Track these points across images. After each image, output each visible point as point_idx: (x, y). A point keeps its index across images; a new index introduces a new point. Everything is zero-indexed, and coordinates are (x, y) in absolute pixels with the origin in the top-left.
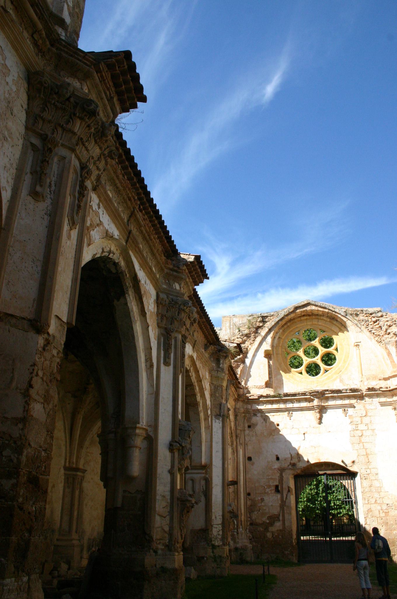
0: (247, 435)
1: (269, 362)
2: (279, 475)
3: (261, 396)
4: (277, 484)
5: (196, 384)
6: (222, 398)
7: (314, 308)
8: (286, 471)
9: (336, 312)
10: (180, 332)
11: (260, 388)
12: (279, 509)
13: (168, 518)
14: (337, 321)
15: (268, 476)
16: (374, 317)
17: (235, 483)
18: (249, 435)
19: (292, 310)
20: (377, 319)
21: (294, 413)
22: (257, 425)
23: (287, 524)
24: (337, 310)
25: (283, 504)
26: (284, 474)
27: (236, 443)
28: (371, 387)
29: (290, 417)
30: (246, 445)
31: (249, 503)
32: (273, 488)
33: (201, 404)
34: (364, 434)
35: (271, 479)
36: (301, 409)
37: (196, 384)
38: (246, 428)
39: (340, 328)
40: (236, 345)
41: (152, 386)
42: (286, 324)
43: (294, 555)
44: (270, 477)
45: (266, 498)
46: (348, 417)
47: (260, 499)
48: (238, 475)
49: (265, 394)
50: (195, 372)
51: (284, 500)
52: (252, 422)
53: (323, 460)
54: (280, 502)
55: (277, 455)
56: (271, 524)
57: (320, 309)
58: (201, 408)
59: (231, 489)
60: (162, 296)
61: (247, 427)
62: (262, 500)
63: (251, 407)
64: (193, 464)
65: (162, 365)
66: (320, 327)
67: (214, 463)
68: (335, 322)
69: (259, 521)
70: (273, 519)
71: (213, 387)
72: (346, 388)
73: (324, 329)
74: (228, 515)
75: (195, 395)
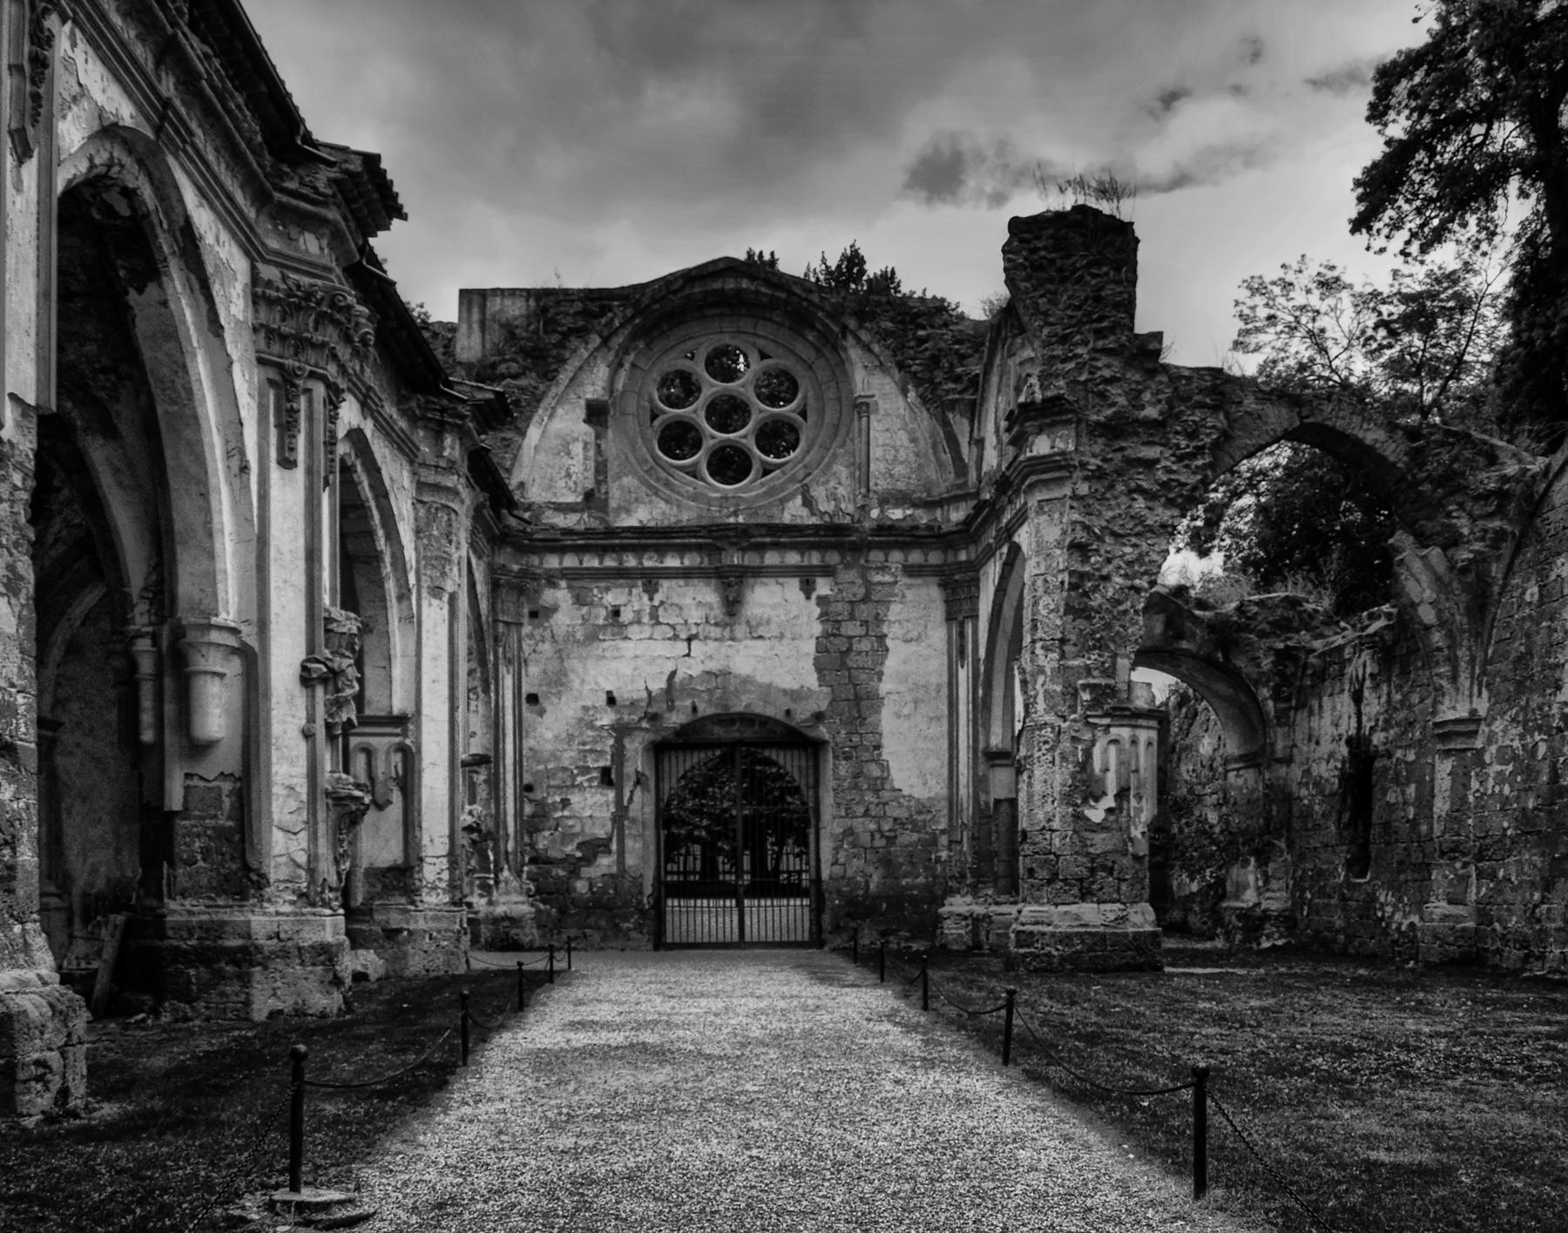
5: (372, 504)
6: (450, 542)
9: (811, 302)
10: (323, 378)
12: (609, 824)
18: (531, 636)
21: (665, 584)
27: (496, 657)
33: (387, 559)
37: (372, 504)
39: (818, 350)
40: (490, 396)
47: (558, 799)
53: (739, 706)
55: (609, 693)
58: (387, 568)
60: (269, 272)
64: (368, 712)
65: (273, 465)
67: (425, 710)
71: (422, 512)
74: (463, 840)
75: (370, 534)
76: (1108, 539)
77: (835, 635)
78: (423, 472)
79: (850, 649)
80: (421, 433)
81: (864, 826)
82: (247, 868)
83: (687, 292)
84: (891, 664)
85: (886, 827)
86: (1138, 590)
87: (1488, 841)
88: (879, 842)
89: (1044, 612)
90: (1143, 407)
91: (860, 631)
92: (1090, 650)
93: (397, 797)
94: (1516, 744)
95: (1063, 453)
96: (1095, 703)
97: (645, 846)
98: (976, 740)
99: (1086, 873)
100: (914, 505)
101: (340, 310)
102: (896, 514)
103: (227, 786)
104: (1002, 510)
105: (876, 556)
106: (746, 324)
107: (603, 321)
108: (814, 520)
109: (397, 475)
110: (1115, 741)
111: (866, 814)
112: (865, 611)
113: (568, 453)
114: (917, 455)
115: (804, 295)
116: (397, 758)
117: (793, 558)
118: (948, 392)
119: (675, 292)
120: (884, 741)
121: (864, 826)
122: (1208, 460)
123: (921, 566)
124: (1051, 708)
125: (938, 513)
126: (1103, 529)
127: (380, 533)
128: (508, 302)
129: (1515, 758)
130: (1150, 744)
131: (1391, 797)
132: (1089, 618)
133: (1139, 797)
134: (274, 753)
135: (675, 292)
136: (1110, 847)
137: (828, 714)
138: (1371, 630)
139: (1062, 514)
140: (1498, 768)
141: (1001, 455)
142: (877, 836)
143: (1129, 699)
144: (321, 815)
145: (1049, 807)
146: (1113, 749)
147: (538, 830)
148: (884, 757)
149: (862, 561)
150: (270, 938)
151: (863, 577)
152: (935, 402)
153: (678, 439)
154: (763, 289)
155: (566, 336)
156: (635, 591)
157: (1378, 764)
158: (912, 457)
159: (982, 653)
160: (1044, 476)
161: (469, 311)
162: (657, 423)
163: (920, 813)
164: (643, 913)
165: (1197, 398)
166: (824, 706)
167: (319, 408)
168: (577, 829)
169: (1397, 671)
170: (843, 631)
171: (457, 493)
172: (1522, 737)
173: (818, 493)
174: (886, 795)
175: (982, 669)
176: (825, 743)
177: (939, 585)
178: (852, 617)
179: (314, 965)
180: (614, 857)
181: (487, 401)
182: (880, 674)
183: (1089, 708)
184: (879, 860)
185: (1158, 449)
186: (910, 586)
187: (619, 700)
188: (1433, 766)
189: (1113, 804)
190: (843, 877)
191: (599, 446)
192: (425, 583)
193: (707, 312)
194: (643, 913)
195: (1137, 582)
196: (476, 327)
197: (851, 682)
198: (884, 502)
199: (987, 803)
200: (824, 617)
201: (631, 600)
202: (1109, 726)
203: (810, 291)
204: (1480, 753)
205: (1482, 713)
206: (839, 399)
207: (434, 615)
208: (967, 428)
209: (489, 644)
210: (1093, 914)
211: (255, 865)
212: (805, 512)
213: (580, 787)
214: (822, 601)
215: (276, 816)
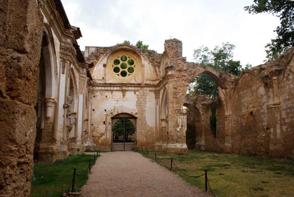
1: (105, 69)
2: (105, 117)
3: (100, 84)
4: (104, 121)
5: (73, 79)
7: (127, 47)
8: (109, 116)
10: (69, 60)
11: (100, 80)
12: (105, 130)
13: (62, 133)
14: (136, 54)
17: (87, 120)
19: (117, 47)
21: (114, 92)
22: (97, 96)
23: (108, 137)
24: (137, 50)
26: (107, 117)
28: (146, 83)
29: (112, 93)
31: (92, 128)
32: (103, 122)
33: (75, 88)
34: (142, 103)
36: (117, 90)
37: (73, 79)
38: (93, 97)
40: (91, 63)
41: (57, 82)
45: (99, 126)
46: (136, 95)
48: (88, 117)
49: (102, 83)
50: (73, 75)
53: (124, 112)
54: (105, 128)
56: (101, 137)
57: (129, 48)
59: (86, 122)
60: (63, 44)
65: (61, 74)
66: (129, 56)
67: (79, 112)
68: (136, 55)
69: (96, 135)
70: (102, 134)
72: (137, 83)
73: (130, 56)
74: (84, 133)
76: (179, 87)
78: (80, 74)
80: (80, 68)
81: (143, 131)
82: (53, 138)
83: (118, 48)
84: (147, 105)
85: (146, 131)
86: (183, 95)
87: (233, 134)
88: (145, 134)
89: (170, 98)
90: (184, 68)
91: (142, 100)
92: (177, 104)
93: (74, 126)
94: (236, 119)
95: (173, 74)
96: (178, 112)
97: (110, 134)
98: (159, 117)
99: (177, 139)
100: (150, 81)
101: (72, 50)
103: (51, 125)
105: (145, 88)
106: (127, 53)
107: (106, 52)
109: (77, 74)
110: (181, 118)
111: (143, 129)
112: (143, 97)
113: (100, 71)
116: (74, 120)
117: (133, 88)
119: (117, 48)
120: (146, 118)
121: (143, 131)
122: (193, 76)
123: (151, 90)
124: (172, 113)
126: (179, 85)
127: (74, 84)
128: (93, 48)
129: (236, 121)
130: (186, 118)
131: (219, 127)
132: (177, 99)
133: (184, 127)
134: (59, 119)
135: (117, 48)
136: (180, 135)
138: (215, 101)
140: (234, 122)
141: (163, 74)
143: (183, 112)
144: (65, 130)
145: (171, 128)
146: (180, 119)
147: (93, 131)
148: (146, 120)
149: (143, 89)
150: (56, 150)
151: (143, 92)
152: (154, 66)
153: (116, 70)
155: (101, 54)
156: (109, 93)
158: (150, 74)
161: (87, 50)
162: (113, 67)
163: (151, 129)
164: (109, 145)
165: (191, 67)
166: (137, 112)
167: (68, 64)
168: (100, 131)
169: (219, 107)
170: (140, 100)
171: (85, 78)
172: (237, 118)
173: (137, 79)
174: (146, 126)
175: (160, 106)
176: (137, 118)
178: (141, 98)
179: (63, 154)
180: (105, 136)
181: (90, 64)
182: (145, 107)
183: (177, 113)
184: (145, 137)
186: (150, 93)
187: (106, 110)
188: (224, 122)
189: (181, 128)
190: (140, 139)
191: (105, 70)
192: (80, 92)
193: (121, 51)
194: (109, 145)
195: (183, 94)
196: (87, 52)
198: (146, 80)
200: (137, 98)
201: (108, 94)
202: (180, 116)
203: (136, 48)
204: (231, 120)
205: (231, 114)
207: (81, 97)
208: (158, 70)
209: (87, 101)
210: (179, 146)
211: (54, 138)
214: (137, 95)
215: (58, 130)
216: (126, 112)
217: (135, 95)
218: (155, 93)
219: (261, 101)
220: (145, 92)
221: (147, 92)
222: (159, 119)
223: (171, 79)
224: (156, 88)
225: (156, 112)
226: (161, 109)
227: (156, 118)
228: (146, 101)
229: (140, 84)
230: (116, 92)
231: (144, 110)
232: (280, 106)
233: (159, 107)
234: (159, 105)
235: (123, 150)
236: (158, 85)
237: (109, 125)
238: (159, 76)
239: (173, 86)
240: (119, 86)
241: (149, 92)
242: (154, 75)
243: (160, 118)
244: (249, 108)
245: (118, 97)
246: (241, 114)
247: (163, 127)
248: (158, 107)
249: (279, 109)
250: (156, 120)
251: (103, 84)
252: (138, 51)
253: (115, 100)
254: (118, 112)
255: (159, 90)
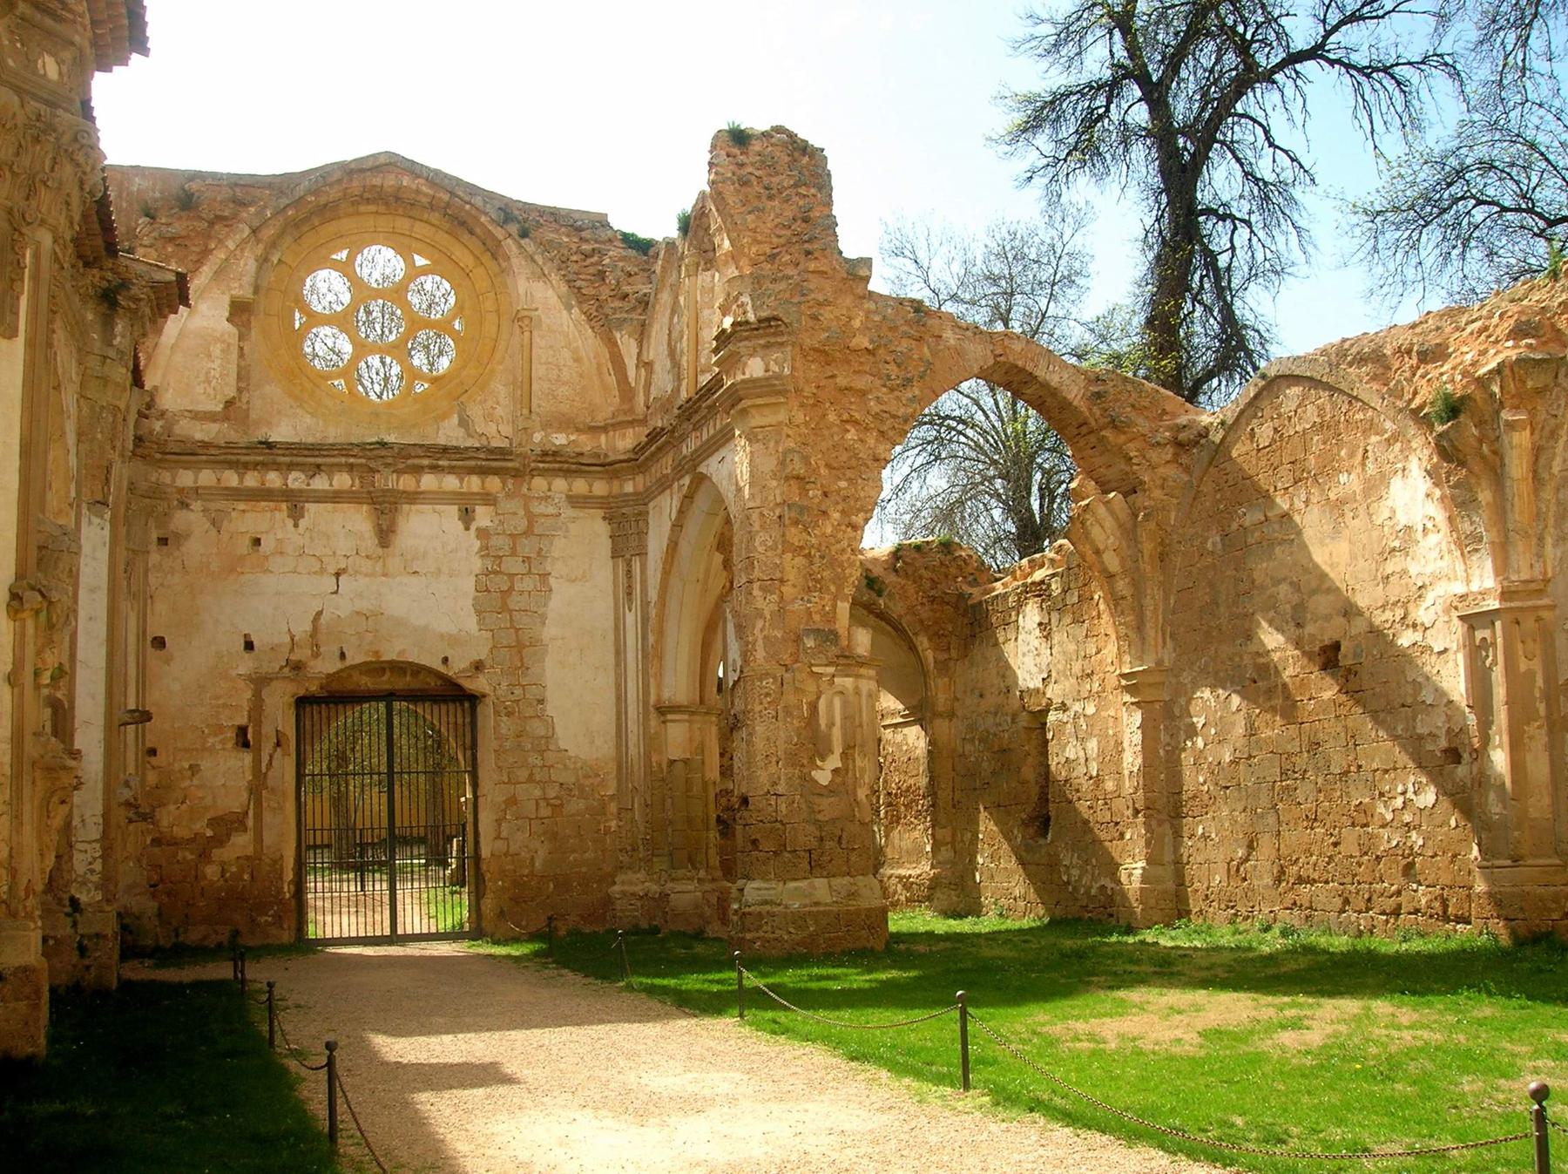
0: (154, 566)
2: (249, 694)
4: (243, 721)
8: (275, 684)
12: (245, 795)
15: (217, 698)
16: (587, 241)
20: (596, 246)
21: (311, 508)
22: (188, 536)
23: (269, 838)
25: (258, 785)
26: (265, 694)
30: (149, 601)
31: (152, 778)
32: (231, 734)
35: (225, 706)
36: (335, 497)
38: (153, 547)
42: (307, 219)
43: (285, 926)
44: (221, 702)
45: (205, 765)
51: (264, 770)
52: (172, 527)
56: (220, 841)
61: (155, 540)
62: (194, 769)
63: (174, 480)
68: (466, 237)
69: (181, 832)
70: (227, 825)
77: (496, 573)
79: (511, 588)
84: (555, 605)
85: (552, 793)
88: (545, 812)
91: (522, 569)
100: (578, 430)
102: (560, 439)
104: (683, 438)
105: (539, 483)
108: (469, 443)
111: (531, 779)
112: (527, 547)
114: (581, 376)
115: (467, 198)
117: (451, 482)
118: (615, 309)
120: (548, 694)
123: (586, 497)
125: (603, 438)
137: (488, 663)
139: (777, 443)
142: (543, 804)
149: (525, 490)
151: (526, 507)
152: (603, 323)
154: (424, 189)
157: (1052, 717)
159: (653, 595)
160: (759, 401)
163: (587, 777)
166: (484, 652)
168: (208, 801)
173: (475, 412)
174: (551, 757)
175: (653, 612)
176: (484, 696)
177: (604, 518)
178: (514, 553)
182: (543, 618)
184: (545, 833)
185: (870, 378)
186: (574, 519)
187: (256, 643)
190: (506, 854)
191: (241, 349)
197: (512, 627)
198: (547, 426)
199: (660, 765)
200: (485, 551)
201: (270, 522)
206: (498, 311)
208: (635, 351)
212: (461, 432)
213: (211, 750)
214: (483, 533)
216: (402, 652)
217: (467, 529)
218: (608, 519)
219: (1405, 572)
220: (538, 508)
221: (551, 510)
222: (646, 703)
223: (766, 411)
224: (616, 483)
225: (619, 652)
226: (661, 633)
227: (620, 699)
228: (545, 576)
229: (502, 453)
230: (330, 506)
231: (536, 642)
232: (1544, 602)
233: (645, 619)
234: (645, 604)
235: (387, 932)
236: (637, 461)
237: (279, 750)
238: (641, 399)
239: (782, 463)
240: (351, 468)
241: (568, 512)
242: (605, 387)
243: (653, 699)
244: (1309, 616)
245: (344, 546)
246: (1247, 660)
247: (672, 762)
248: (630, 618)
249: (1538, 619)
250: (618, 714)
251: (230, 446)
252: (486, 214)
253: (322, 571)
254: (343, 656)
255: (643, 499)
